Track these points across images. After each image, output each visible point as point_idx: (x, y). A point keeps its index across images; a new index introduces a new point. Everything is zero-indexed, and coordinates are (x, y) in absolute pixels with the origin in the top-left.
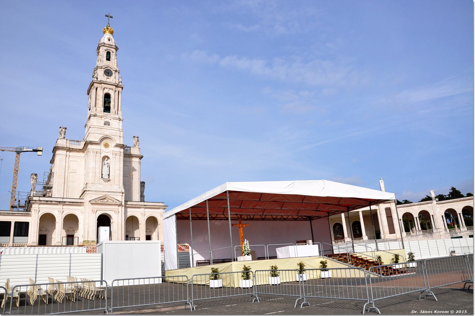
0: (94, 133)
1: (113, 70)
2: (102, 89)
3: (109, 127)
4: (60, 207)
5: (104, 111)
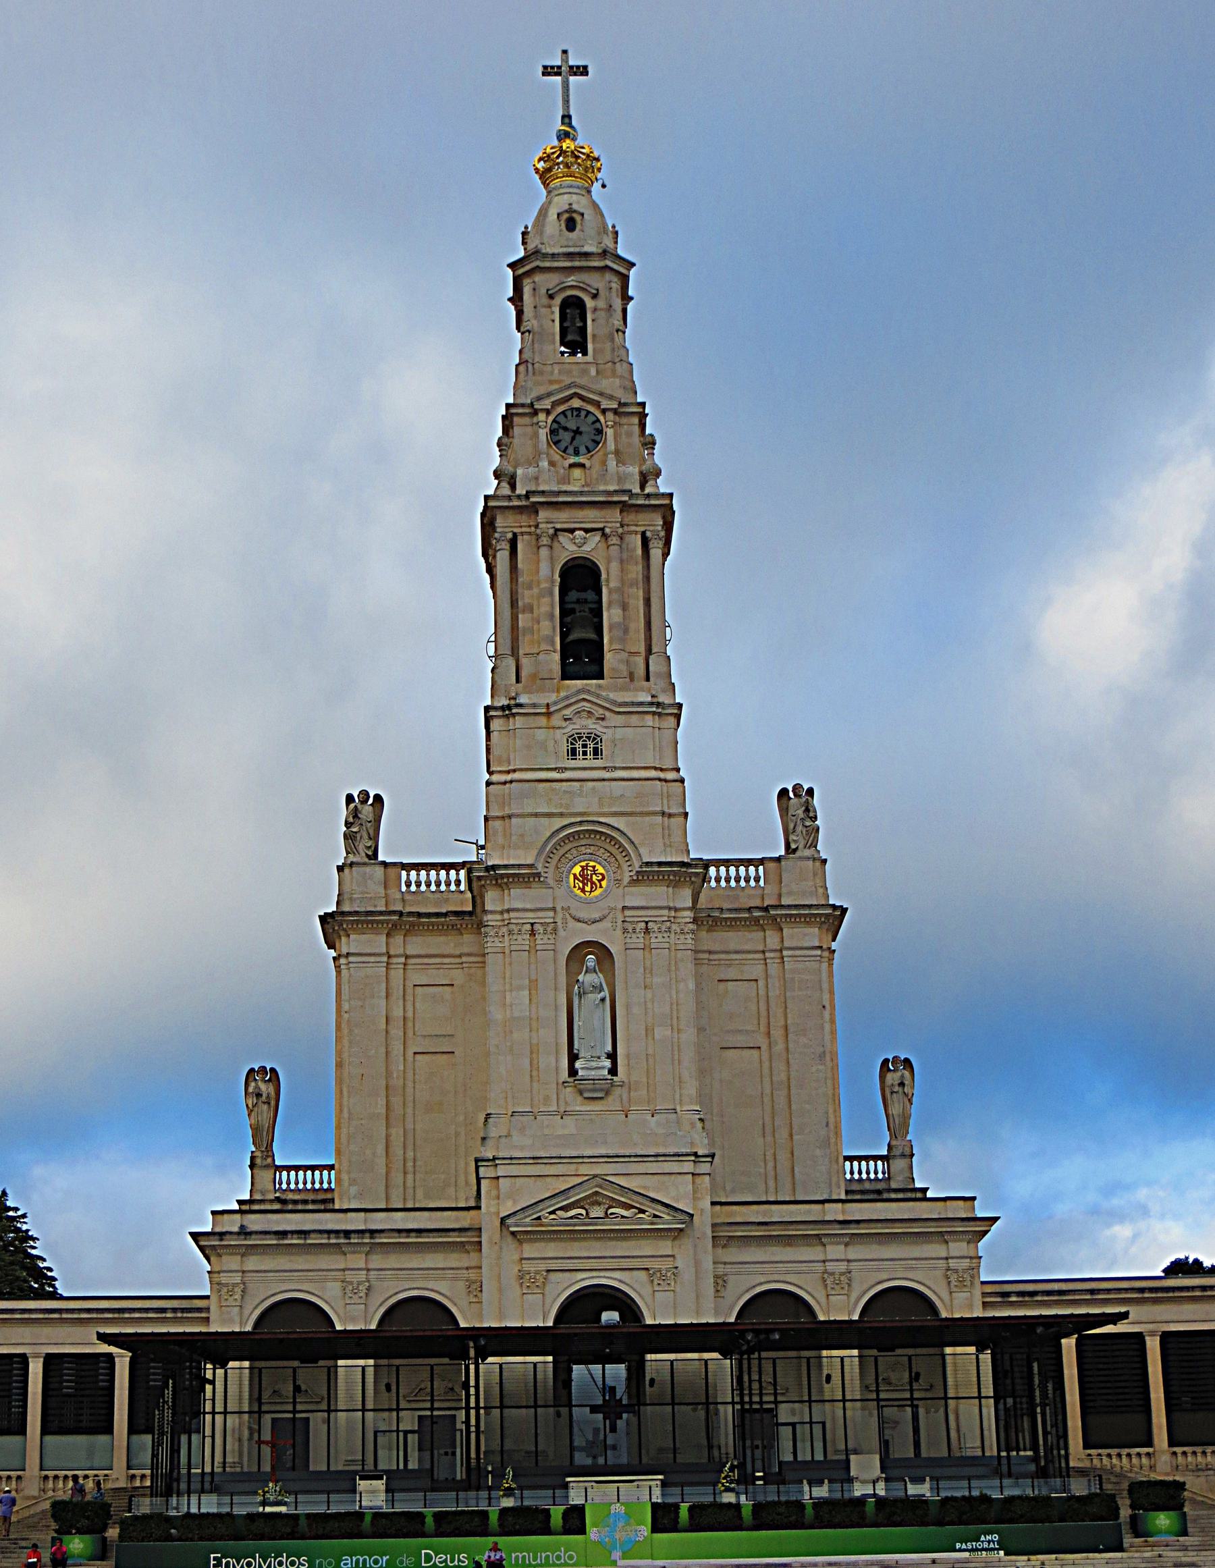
0: (510, 817)
1: (604, 411)
2: (545, 540)
3: (598, 763)
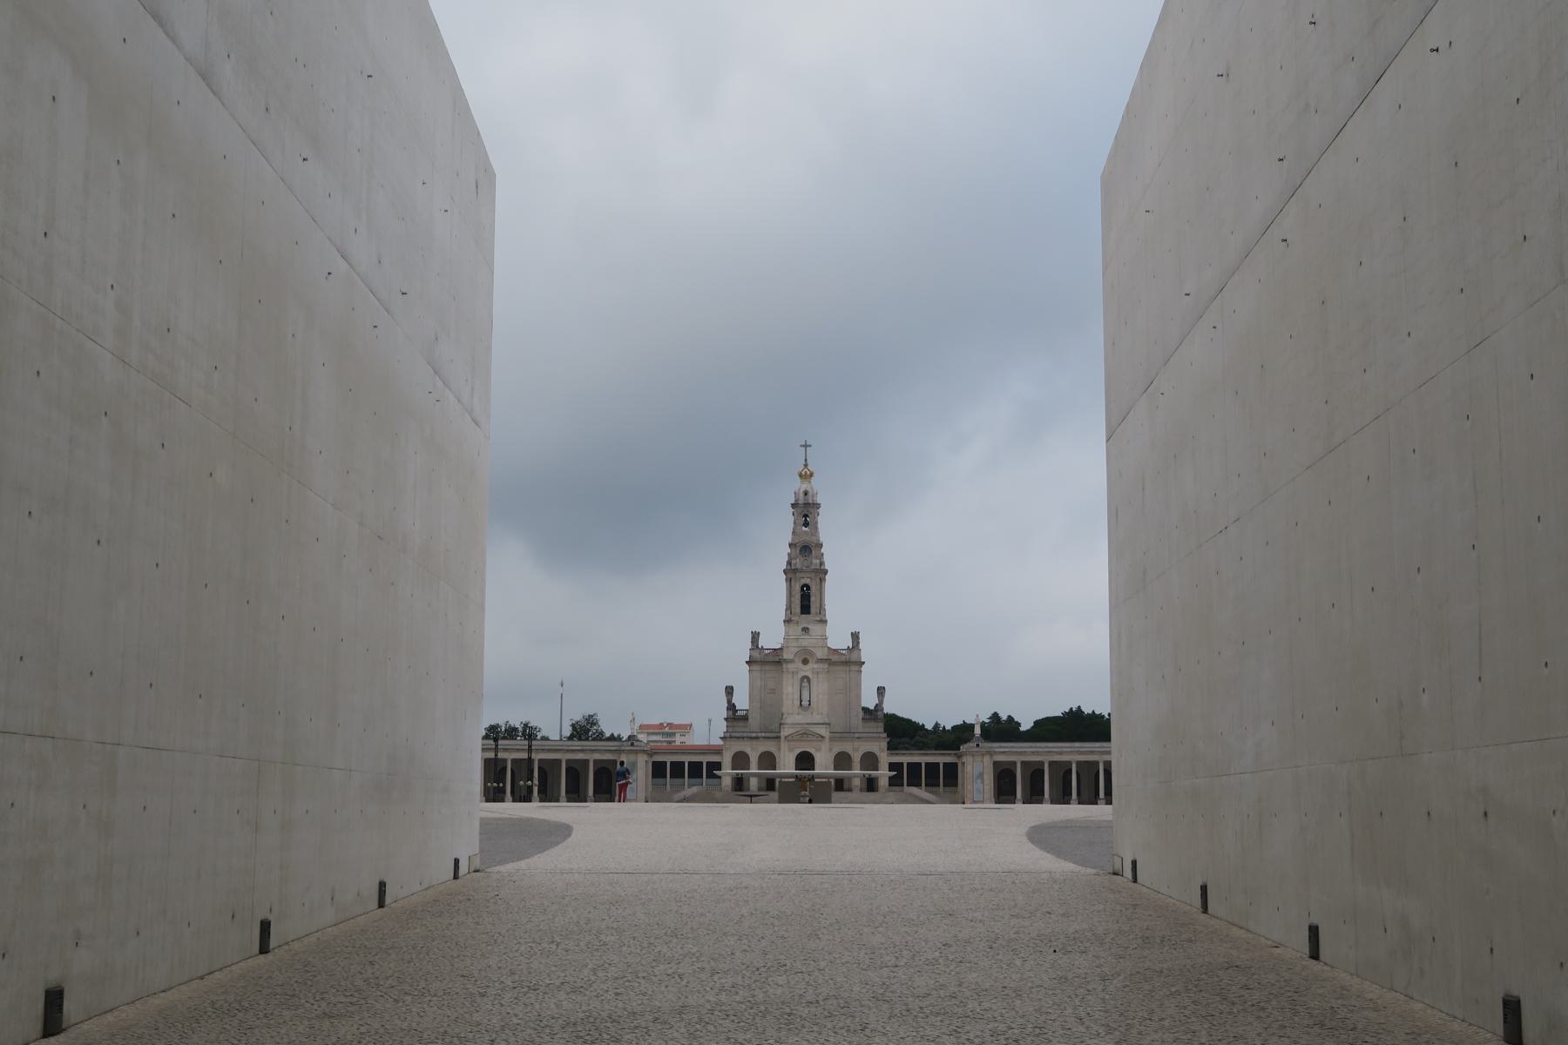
4: (754, 742)
5: (802, 613)
